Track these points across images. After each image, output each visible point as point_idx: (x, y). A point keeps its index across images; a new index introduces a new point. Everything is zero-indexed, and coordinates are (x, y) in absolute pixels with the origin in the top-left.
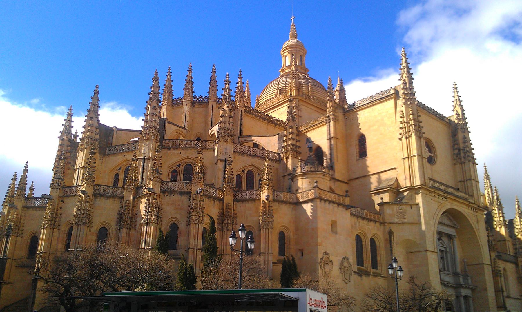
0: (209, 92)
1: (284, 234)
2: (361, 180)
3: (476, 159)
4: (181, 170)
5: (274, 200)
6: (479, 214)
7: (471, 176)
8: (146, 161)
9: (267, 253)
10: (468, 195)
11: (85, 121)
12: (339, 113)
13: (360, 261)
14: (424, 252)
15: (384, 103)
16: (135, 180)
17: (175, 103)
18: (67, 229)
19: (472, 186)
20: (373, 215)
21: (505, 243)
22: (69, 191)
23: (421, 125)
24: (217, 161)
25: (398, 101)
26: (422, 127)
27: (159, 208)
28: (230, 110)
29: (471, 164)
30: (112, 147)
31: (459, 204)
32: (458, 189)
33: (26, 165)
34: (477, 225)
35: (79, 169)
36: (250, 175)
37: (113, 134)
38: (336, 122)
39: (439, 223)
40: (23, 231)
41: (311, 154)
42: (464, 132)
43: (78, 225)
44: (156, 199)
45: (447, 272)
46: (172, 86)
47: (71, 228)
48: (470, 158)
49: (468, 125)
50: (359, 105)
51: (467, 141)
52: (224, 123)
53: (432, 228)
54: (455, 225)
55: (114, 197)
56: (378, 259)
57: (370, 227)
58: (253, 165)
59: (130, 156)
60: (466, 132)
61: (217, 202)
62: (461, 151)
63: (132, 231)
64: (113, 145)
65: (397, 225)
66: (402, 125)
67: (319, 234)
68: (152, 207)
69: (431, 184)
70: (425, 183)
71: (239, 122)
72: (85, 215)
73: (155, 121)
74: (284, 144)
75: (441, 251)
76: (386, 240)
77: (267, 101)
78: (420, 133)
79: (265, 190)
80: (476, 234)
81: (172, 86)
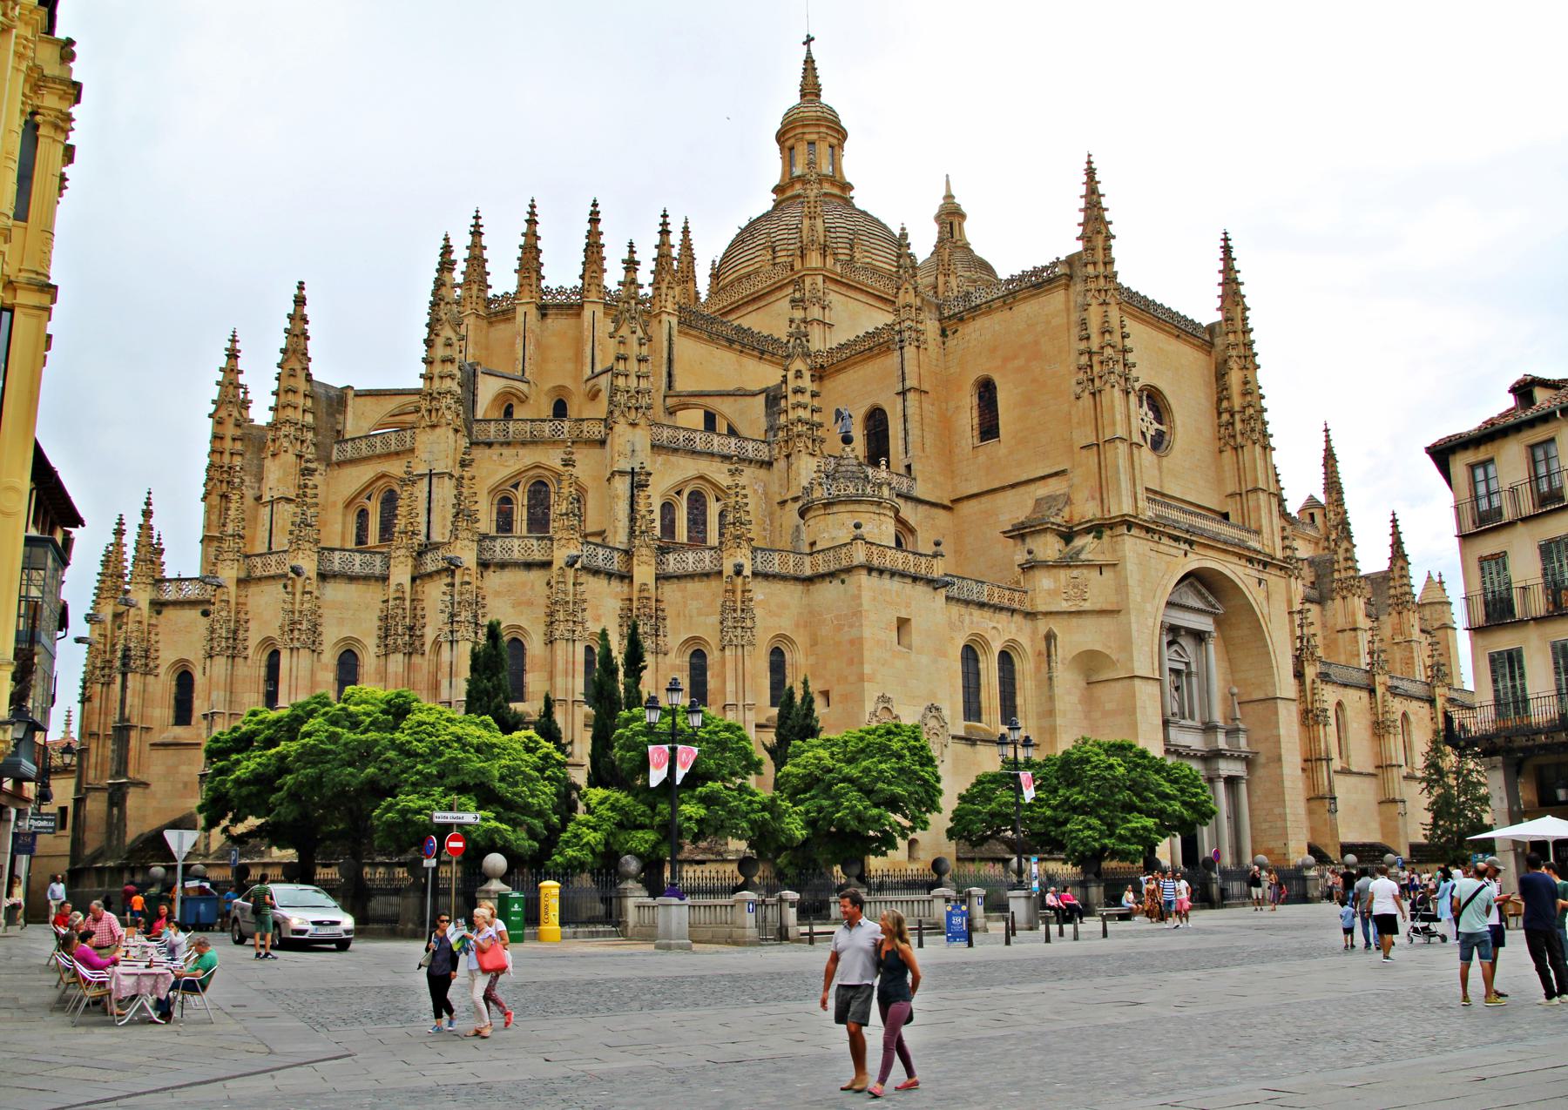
0: (582, 277)
1: (782, 653)
2: (984, 499)
3: (1271, 436)
4: (521, 497)
5: (755, 574)
6: (1273, 577)
7: (1256, 480)
8: (434, 480)
9: (741, 704)
10: (1249, 532)
11: (277, 379)
12: (928, 322)
13: (972, 710)
14: (1128, 681)
15: (1043, 299)
16: (413, 533)
17: (499, 312)
18: (265, 657)
19: (1258, 508)
20: (1007, 592)
21: (1356, 637)
22: (259, 565)
23: (1131, 358)
24: (613, 474)
25: (1072, 297)
26: (1134, 365)
27: (478, 603)
28: (640, 339)
29: (1257, 447)
30: (347, 441)
31: (1222, 556)
32: (1226, 516)
33: (149, 498)
34: (1265, 603)
35: (272, 502)
36: (697, 500)
37: (346, 406)
38: (918, 347)
39: (1170, 604)
40: (158, 662)
41: (848, 449)
42: (1245, 368)
43: (292, 649)
44: (469, 583)
45: (1188, 722)
46: (486, 261)
47: (275, 654)
48: (1256, 436)
49: (1256, 348)
50: (978, 302)
51: (1251, 391)
52: (627, 376)
53: (1150, 622)
54: (1213, 606)
55: (366, 578)
56: (1019, 701)
57: (999, 626)
58: (701, 477)
59: (396, 468)
60: (1250, 366)
61: (616, 585)
62: (1237, 417)
63: (416, 659)
64: (347, 436)
65: (1066, 617)
66: (1084, 359)
67: (866, 654)
68: (459, 603)
69: (1148, 512)
70: (1137, 507)
71: (665, 355)
72: (305, 622)
73: (452, 377)
74: (783, 419)
75: (1176, 672)
76: (1040, 654)
77: (739, 279)
78: (1127, 380)
79: (732, 550)
80: (1261, 626)
81: (486, 261)
